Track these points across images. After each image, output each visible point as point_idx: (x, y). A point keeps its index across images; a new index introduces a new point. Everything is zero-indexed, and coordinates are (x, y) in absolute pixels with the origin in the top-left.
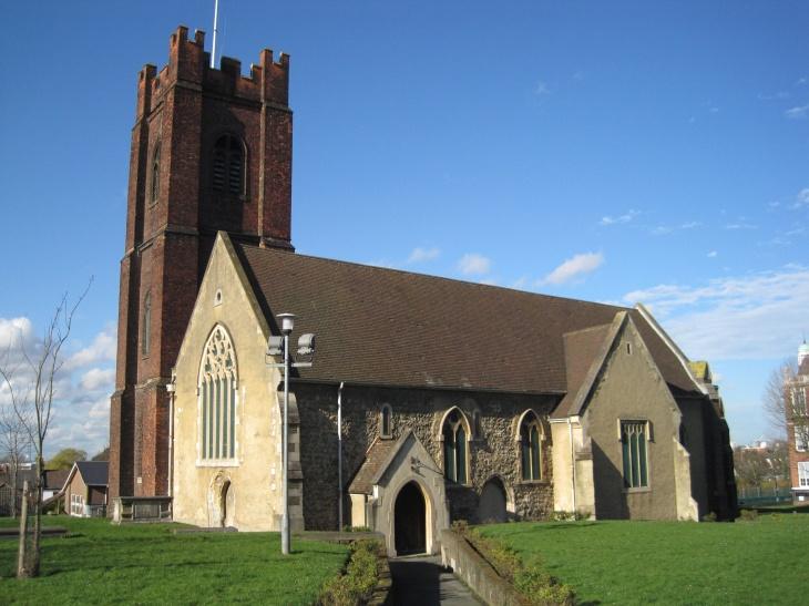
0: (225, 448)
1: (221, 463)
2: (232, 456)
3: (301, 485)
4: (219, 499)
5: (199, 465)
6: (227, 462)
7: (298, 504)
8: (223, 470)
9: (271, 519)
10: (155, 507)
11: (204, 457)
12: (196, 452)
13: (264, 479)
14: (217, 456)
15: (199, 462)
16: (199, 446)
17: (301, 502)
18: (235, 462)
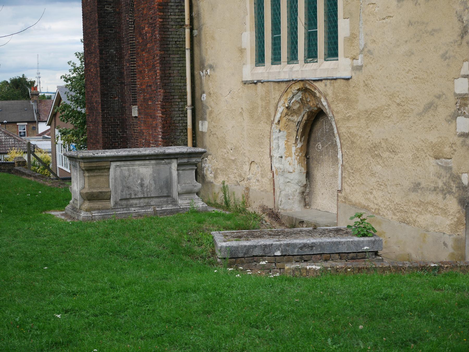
0: (311, 38)
1: (302, 70)
2: (332, 52)
4: (295, 149)
5: (248, 77)
6: (321, 68)
8: (306, 88)
9: (453, 205)
10: (163, 167)
11: (260, 60)
12: (242, 51)
13: (430, 106)
14: (293, 57)
15: (250, 71)
16: (248, 39)
18: (341, 66)
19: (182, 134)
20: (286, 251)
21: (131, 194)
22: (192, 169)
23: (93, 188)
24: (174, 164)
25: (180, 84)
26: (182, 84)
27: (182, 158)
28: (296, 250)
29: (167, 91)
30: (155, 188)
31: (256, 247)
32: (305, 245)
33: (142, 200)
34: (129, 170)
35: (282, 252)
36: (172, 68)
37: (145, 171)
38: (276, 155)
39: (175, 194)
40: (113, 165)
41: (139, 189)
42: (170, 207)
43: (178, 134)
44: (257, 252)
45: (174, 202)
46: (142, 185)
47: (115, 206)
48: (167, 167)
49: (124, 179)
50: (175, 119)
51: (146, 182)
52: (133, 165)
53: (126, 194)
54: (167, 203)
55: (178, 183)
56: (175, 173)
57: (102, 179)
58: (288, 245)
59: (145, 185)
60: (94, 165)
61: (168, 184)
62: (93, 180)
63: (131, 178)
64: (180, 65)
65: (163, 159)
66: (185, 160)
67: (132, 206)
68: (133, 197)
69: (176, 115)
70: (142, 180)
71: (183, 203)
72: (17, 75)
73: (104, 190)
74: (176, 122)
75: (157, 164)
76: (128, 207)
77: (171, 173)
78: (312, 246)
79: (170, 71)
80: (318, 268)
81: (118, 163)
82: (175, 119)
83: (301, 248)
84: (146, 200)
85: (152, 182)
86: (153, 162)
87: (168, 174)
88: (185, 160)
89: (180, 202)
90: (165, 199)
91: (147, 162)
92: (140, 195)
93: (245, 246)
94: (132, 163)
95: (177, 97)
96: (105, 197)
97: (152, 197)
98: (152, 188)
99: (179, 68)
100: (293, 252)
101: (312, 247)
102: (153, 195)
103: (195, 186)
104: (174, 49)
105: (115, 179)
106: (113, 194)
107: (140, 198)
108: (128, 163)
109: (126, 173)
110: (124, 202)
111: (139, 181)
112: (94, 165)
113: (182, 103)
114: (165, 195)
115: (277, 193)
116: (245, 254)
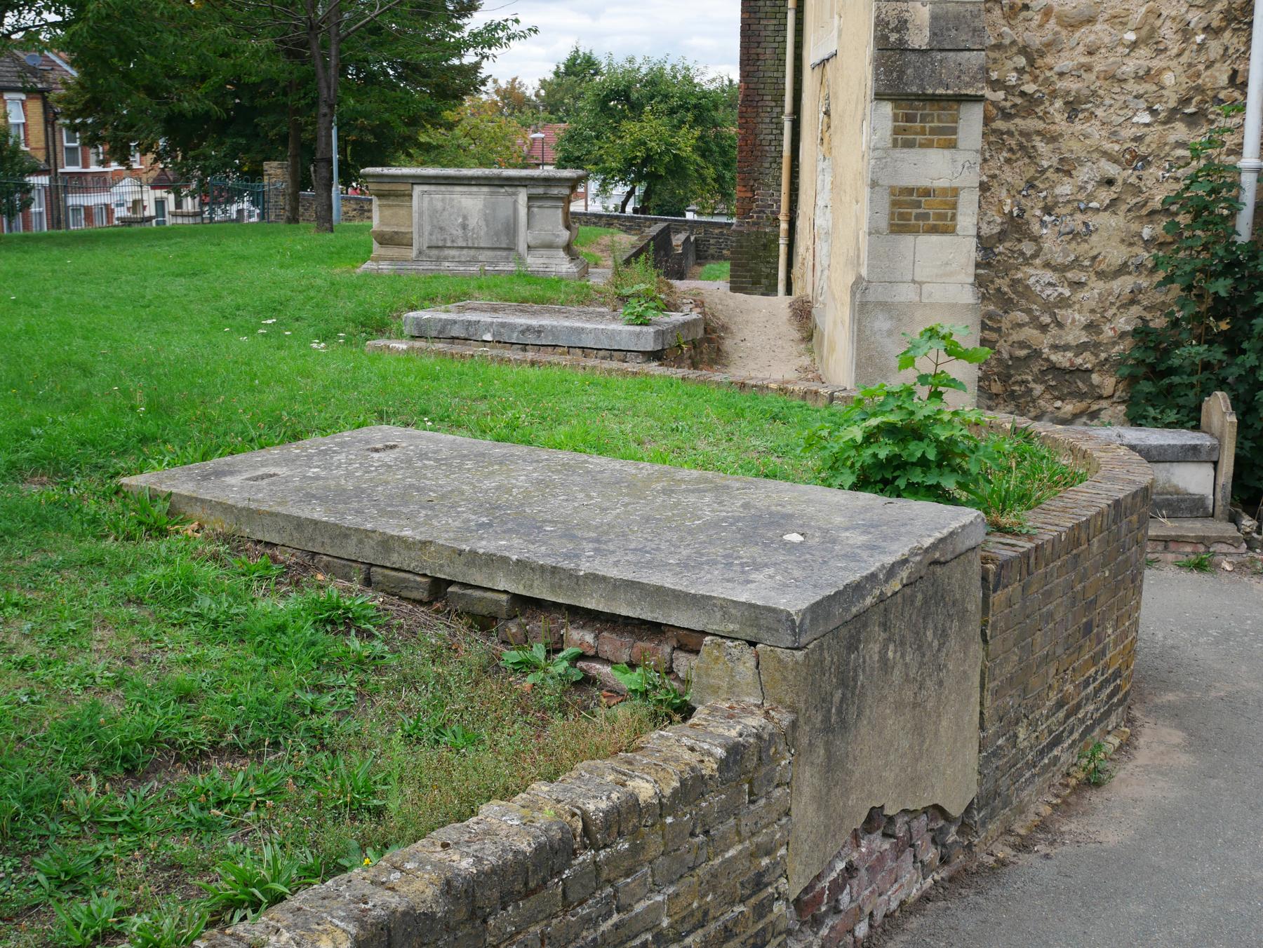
3: (971, 122)
7: (944, 226)
10: (503, 198)
17: (967, 219)
19: (774, 165)
20: (501, 334)
21: (445, 240)
22: (557, 207)
23: (388, 225)
24: (522, 195)
25: (775, 74)
26: (780, 75)
27: (534, 186)
28: (515, 335)
29: (751, 86)
30: (487, 233)
31: (455, 322)
32: (528, 329)
33: (465, 252)
34: (443, 200)
35: (494, 335)
36: (763, 45)
37: (471, 203)
38: (821, 203)
39: (522, 247)
40: (418, 190)
41: (460, 232)
42: (511, 267)
43: (767, 165)
44: (456, 331)
45: (521, 259)
46: (464, 227)
47: (418, 256)
48: (510, 199)
49: (434, 213)
50: (762, 137)
51: (472, 222)
52: (452, 193)
53: (437, 239)
54: (507, 260)
55: (529, 226)
56: (523, 211)
57: (402, 212)
58: (503, 325)
59: (470, 227)
60: (386, 187)
61: (511, 230)
62: (388, 212)
63: (446, 213)
64: (778, 39)
65: (502, 186)
66: (540, 191)
67: (446, 259)
68: (449, 244)
69: (765, 129)
70: (465, 218)
71: (534, 262)
72: (564, 55)
73: (403, 230)
74: (764, 143)
75: (492, 194)
76: (439, 260)
77: (515, 210)
78: (539, 331)
79: (759, 51)
80: (405, 347)
81: (426, 188)
82: (762, 137)
83: (523, 332)
84: (472, 252)
85: (482, 223)
86: (485, 189)
87: (510, 212)
88: (540, 191)
89: (530, 260)
90: (504, 254)
91: (475, 189)
92: (461, 243)
93: (440, 320)
94: (449, 188)
95: (769, 98)
96: (405, 241)
97: (483, 248)
98: (482, 233)
99: (776, 45)
100: (510, 337)
101: (539, 332)
102: (482, 245)
103: (558, 236)
104: (769, 9)
105: (421, 214)
106: (415, 236)
107: (462, 248)
108: (443, 188)
109: (439, 205)
110: (434, 252)
111: (460, 220)
112: (386, 187)
113: (779, 110)
114: (504, 246)
115: (818, 273)
116: (440, 332)
